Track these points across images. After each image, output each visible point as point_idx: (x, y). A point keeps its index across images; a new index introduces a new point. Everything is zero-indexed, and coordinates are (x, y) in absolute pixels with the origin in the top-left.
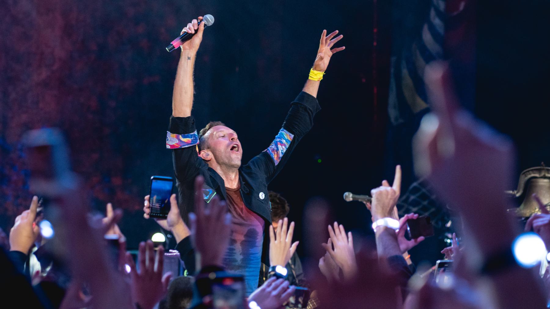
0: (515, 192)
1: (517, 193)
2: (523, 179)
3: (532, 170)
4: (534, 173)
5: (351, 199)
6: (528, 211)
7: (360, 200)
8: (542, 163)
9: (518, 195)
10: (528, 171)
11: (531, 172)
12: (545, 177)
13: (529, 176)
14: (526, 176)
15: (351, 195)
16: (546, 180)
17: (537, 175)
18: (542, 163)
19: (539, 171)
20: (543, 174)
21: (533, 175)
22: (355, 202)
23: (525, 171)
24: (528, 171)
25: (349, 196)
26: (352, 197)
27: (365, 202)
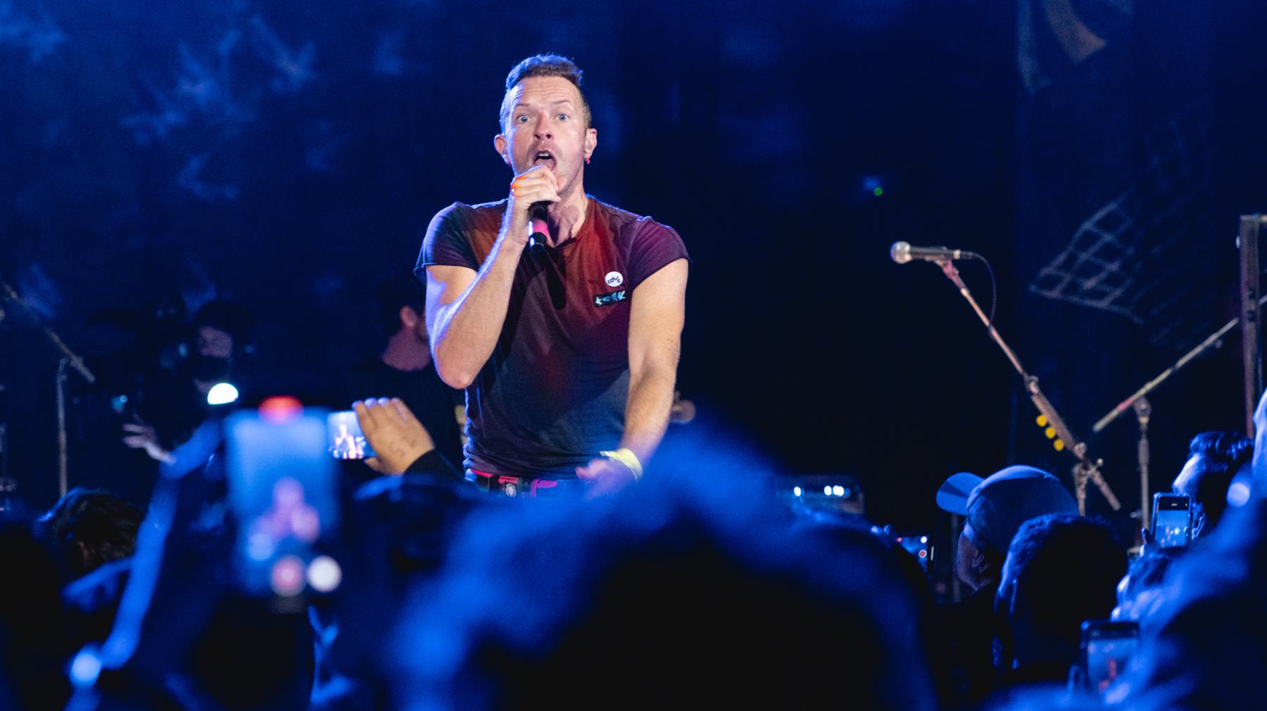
5: (908, 258)
7: (928, 258)
15: (907, 248)
22: (916, 264)
25: (903, 252)
26: (911, 253)
27: (939, 263)
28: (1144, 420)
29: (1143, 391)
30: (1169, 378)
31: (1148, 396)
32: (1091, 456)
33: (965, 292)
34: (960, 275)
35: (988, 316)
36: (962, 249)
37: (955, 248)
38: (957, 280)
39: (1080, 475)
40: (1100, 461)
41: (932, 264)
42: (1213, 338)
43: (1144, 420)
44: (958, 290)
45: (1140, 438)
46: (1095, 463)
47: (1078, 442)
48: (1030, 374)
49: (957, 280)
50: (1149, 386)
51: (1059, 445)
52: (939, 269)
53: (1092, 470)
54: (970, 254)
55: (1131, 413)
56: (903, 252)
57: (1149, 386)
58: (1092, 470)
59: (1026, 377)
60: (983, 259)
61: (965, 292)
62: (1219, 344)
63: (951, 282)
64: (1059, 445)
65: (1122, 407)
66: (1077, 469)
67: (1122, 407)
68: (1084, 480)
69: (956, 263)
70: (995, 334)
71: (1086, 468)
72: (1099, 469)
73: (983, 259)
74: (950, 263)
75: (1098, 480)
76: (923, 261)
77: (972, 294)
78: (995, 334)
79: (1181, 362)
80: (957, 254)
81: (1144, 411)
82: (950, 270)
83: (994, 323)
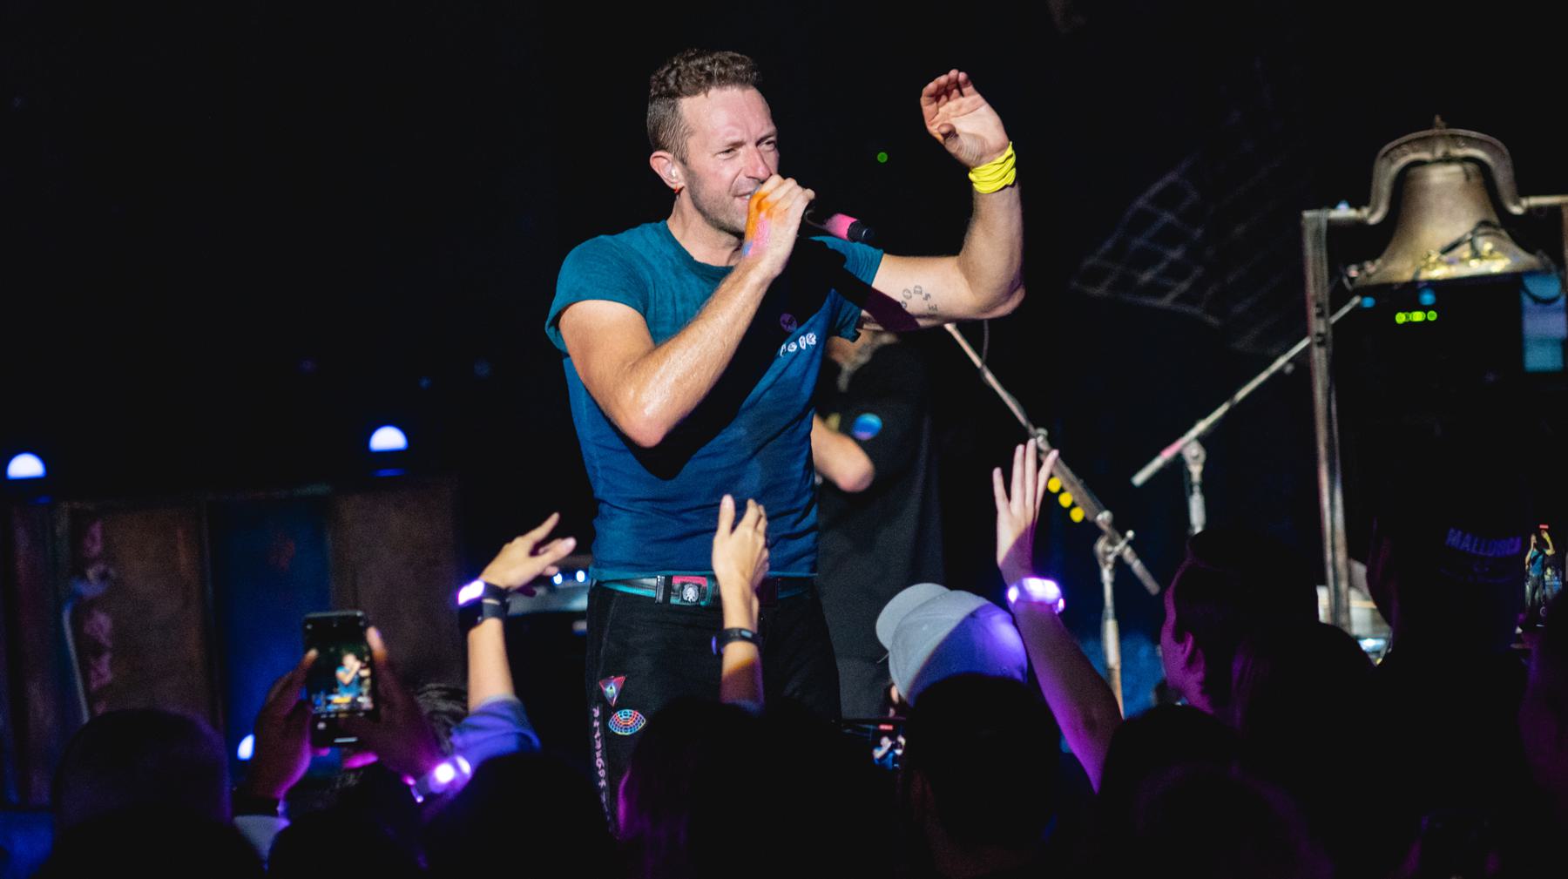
0: (1365, 212)
2: (1386, 173)
3: (1407, 143)
4: (1415, 151)
6: (1409, 264)
8: (1438, 119)
10: (1398, 146)
11: (1405, 148)
12: (1448, 160)
13: (1402, 162)
14: (1392, 162)
16: (1455, 168)
17: (1425, 156)
18: (1438, 119)
19: (1426, 142)
20: (1439, 153)
21: (1413, 157)
23: (1387, 147)
24: (1398, 146)
28: (1196, 470)
30: (1227, 414)
31: (1202, 440)
32: (1119, 526)
35: (978, 352)
39: (1106, 553)
40: (1130, 534)
42: (1281, 361)
43: (1196, 470)
45: (1192, 492)
46: (1123, 536)
47: (1101, 511)
48: (1036, 426)
50: (1201, 426)
51: (1077, 515)
53: (1122, 544)
55: (1179, 462)
57: (1201, 426)
58: (1122, 544)
62: (1289, 368)
64: (1077, 515)
66: (1101, 546)
67: (1168, 454)
68: (1111, 558)
70: (990, 377)
71: (1112, 543)
72: (1130, 543)
75: (1128, 553)
78: (990, 377)
79: (1241, 394)
81: (1196, 457)
83: (988, 363)
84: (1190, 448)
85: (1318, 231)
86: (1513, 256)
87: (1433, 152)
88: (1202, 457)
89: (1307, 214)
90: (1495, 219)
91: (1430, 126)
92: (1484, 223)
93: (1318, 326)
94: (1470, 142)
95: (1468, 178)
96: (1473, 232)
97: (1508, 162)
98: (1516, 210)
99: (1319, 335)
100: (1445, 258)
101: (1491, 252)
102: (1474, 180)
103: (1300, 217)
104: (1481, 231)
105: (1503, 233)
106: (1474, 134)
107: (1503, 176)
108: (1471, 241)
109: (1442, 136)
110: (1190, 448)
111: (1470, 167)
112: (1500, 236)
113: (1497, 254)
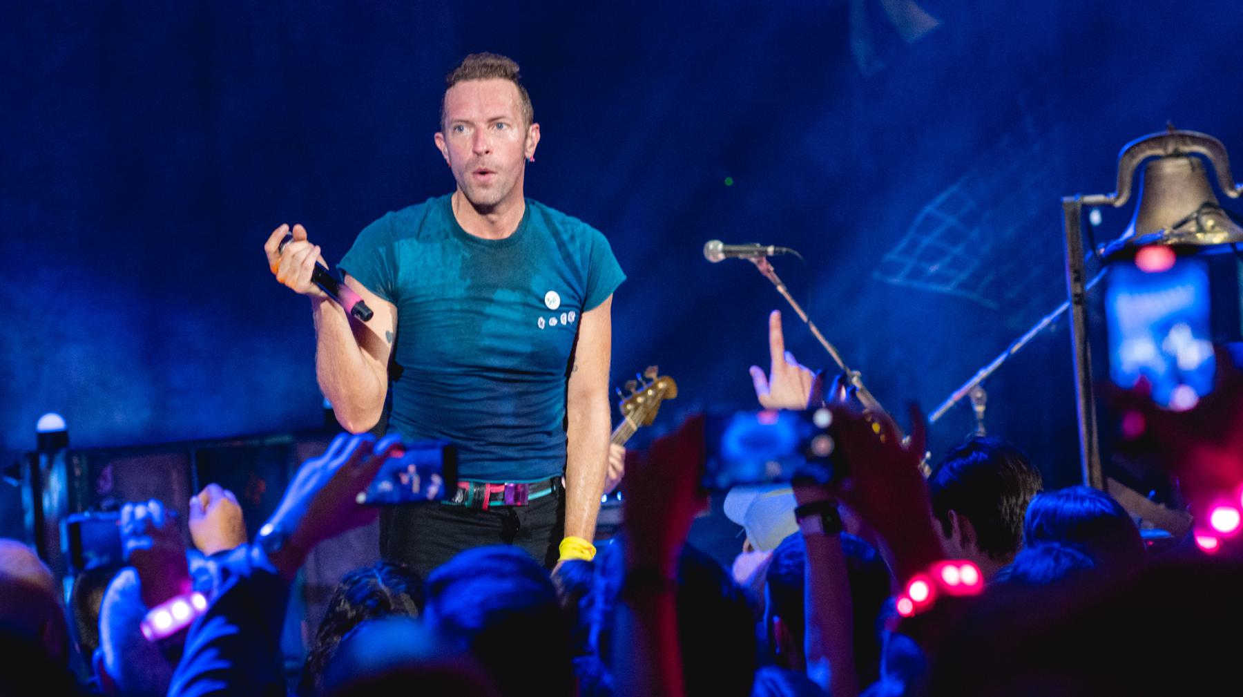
0: (1112, 197)
1: (1118, 198)
2: (1128, 166)
4: (1152, 148)
5: (721, 257)
7: (741, 256)
8: (1168, 122)
9: (1119, 203)
10: (1138, 145)
11: (1143, 146)
12: (1177, 155)
13: (1141, 157)
14: (1133, 157)
15: (720, 246)
16: (1183, 162)
17: (1159, 152)
19: (1160, 141)
20: (1170, 149)
21: (1149, 153)
22: (731, 263)
23: (1127, 147)
24: (1138, 145)
25: (715, 250)
26: (724, 252)
27: (753, 260)
28: (980, 409)
29: (976, 380)
31: (985, 384)
33: (781, 289)
34: (775, 271)
36: (776, 246)
37: (768, 245)
38: (773, 277)
41: (746, 262)
42: (1046, 321)
43: (980, 409)
44: (774, 287)
48: (852, 369)
49: (773, 277)
50: (983, 374)
52: (753, 267)
54: (784, 250)
55: (966, 404)
56: (715, 250)
57: (983, 374)
59: (848, 371)
60: (796, 253)
61: (781, 289)
62: (1053, 328)
63: (766, 278)
65: (957, 396)
67: (957, 396)
69: (770, 260)
70: (814, 329)
73: (796, 253)
74: (764, 260)
76: (737, 260)
77: (789, 290)
78: (814, 329)
80: (771, 250)
81: (978, 399)
82: (765, 267)
84: (973, 387)
85: (1074, 213)
86: (1231, 231)
87: (1165, 149)
88: (985, 399)
89: (1066, 199)
90: (1216, 202)
91: (1162, 128)
92: (1206, 205)
93: (1073, 288)
94: (1195, 140)
95: (1193, 169)
96: (1198, 212)
97: (1226, 156)
98: (1233, 194)
99: (1076, 295)
100: (1176, 232)
101: (1213, 227)
102: (1199, 171)
103: (1061, 203)
104: (1205, 210)
105: (1223, 212)
106: (1198, 134)
107: (1221, 167)
108: (1197, 219)
109: (1173, 136)
110: (973, 387)
111: (1195, 160)
112: (1219, 214)
113: (1217, 229)
